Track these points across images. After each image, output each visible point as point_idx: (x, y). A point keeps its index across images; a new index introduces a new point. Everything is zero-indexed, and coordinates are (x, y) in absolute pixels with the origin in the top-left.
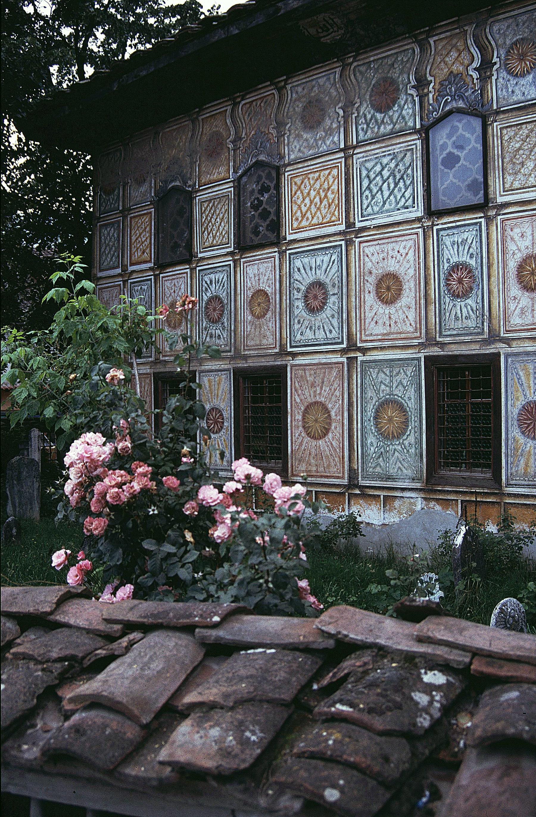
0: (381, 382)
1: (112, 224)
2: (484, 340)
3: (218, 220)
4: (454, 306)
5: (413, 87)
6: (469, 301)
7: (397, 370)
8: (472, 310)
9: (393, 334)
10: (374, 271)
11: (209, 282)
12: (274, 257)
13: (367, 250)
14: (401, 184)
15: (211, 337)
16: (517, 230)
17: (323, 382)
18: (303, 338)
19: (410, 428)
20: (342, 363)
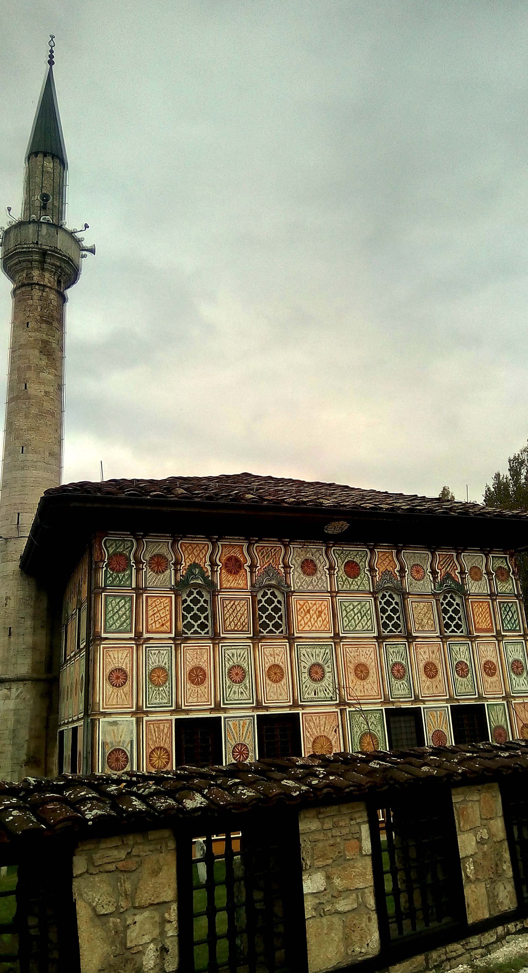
1: (123, 597)
11: (231, 655)
13: (347, 649)
14: (365, 618)
15: (235, 693)
18: (309, 696)
20: (337, 712)
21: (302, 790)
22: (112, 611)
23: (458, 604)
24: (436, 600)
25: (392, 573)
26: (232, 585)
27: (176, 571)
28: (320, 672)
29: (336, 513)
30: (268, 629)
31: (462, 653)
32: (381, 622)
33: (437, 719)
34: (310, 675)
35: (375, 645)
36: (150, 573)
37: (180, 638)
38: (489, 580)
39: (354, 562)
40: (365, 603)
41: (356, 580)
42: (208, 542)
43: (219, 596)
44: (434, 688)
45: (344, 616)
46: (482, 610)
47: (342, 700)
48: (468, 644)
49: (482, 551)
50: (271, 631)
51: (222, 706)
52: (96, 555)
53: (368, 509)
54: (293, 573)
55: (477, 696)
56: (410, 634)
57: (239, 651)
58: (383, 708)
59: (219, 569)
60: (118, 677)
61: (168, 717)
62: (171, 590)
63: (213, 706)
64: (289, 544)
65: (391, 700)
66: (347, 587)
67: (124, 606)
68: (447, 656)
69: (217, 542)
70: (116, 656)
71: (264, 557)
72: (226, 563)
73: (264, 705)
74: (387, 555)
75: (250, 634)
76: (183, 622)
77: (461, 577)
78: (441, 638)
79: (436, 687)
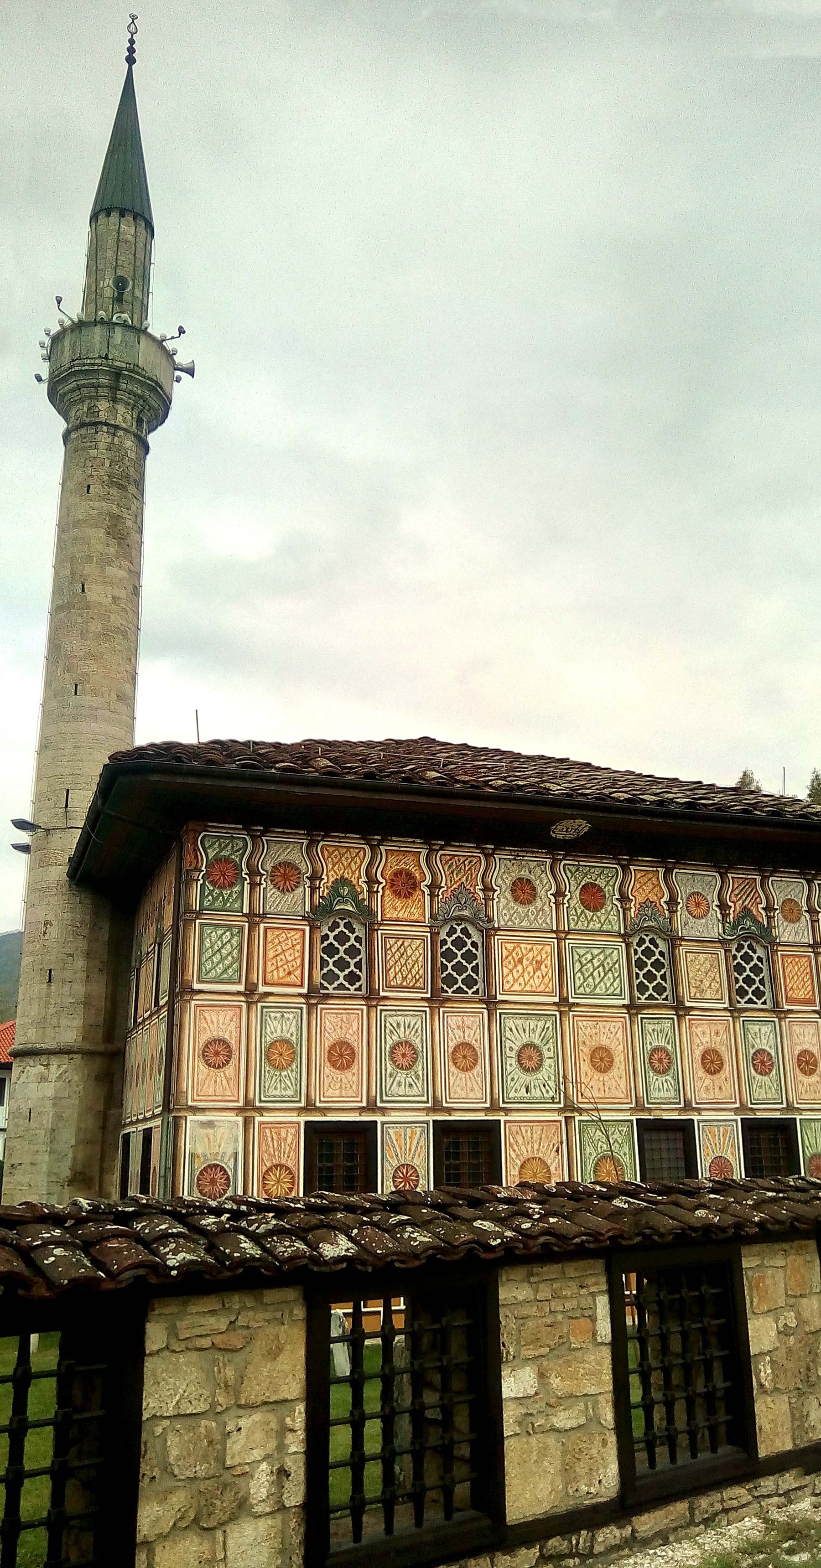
2: (680, 1109)
10: (587, 1043)
11: (395, 1025)
13: (580, 1023)
14: (610, 975)
16: (700, 1029)
17: (541, 1139)
20: (560, 1122)
21: (507, 1237)
22: (211, 948)
23: (760, 959)
24: (726, 951)
26: (400, 915)
27: (313, 889)
28: (536, 1059)
29: (570, 805)
30: (455, 987)
31: (763, 1036)
32: (636, 982)
33: (719, 1139)
34: (519, 1061)
35: (624, 1018)
36: (272, 892)
37: (315, 996)
38: (812, 921)
40: (611, 951)
41: (599, 914)
42: (364, 846)
43: (379, 932)
44: (717, 1090)
45: (576, 970)
46: (799, 969)
47: (569, 1103)
48: (774, 1021)
49: (802, 874)
50: (459, 990)
51: (379, 1104)
52: (188, 858)
53: (622, 801)
54: (497, 900)
55: (784, 1106)
56: (682, 1002)
57: (408, 1020)
58: (634, 1118)
59: (380, 889)
60: (217, 1053)
61: (293, 1117)
62: (304, 918)
63: (364, 1104)
64: (493, 853)
65: (646, 1106)
66: (583, 925)
67: (229, 941)
69: (378, 845)
70: (215, 1020)
71: (452, 873)
73: (445, 1105)
74: (650, 876)
75: (427, 993)
76: (322, 969)
77: (767, 915)
79: (720, 1088)
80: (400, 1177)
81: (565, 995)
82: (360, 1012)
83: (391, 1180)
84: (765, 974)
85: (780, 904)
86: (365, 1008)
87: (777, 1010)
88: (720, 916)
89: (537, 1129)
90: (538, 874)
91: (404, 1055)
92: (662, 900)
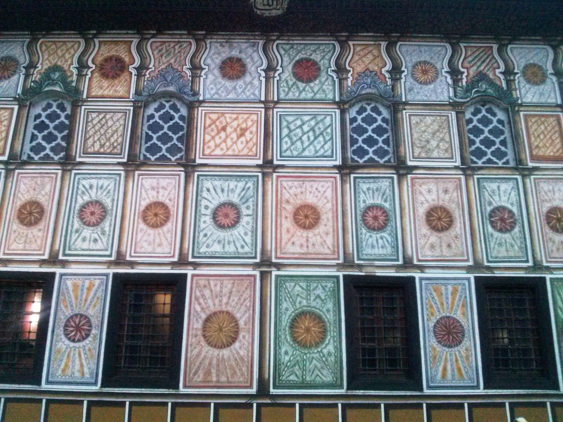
0: (298, 295)
3: (110, 131)
4: (371, 236)
5: (333, 71)
6: (384, 234)
7: (315, 285)
8: (387, 241)
9: (310, 254)
10: (291, 201)
11: (88, 187)
12: (179, 175)
13: (285, 184)
14: (321, 138)
17: (231, 293)
18: (208, 250)
19: (329, 337)
20: (254, 276)
24: (457, 113)
25: (376, 74)
27: (27, 76)
28: (232, 215)
33: (447, 298)
35: (335, 178)
39: (310, 60)
41: (312, 84)
46: (546, 128)
48: (516, 179)
51: (61, 257)
54: (205, 77)
55: (531, 264)
56: (404, 162)
57: (101, 182)
59: (89, 73)
62: (15, 99)
63: (46, 257)
65: (356, 262)
66: (294, 95)
68: (473, 197)
71: (161, 56)
72: (102, 65)
73: (128, 258)
74: (370, 48)
75: (123, 158)
77: (506, 79)
78: (462, 169)
79: (449, 246)
80: (72, 327)
81: (270, 158)
82: (54, 176)
83: (62, 329)
84: (507, 134)
85: (521, 68)
86: (60, 172)
87: (521, 168)
88: (450, 81)
89: (228, 284)
90: (249, 53)
91: (92, 213)
92: (383, 71)
